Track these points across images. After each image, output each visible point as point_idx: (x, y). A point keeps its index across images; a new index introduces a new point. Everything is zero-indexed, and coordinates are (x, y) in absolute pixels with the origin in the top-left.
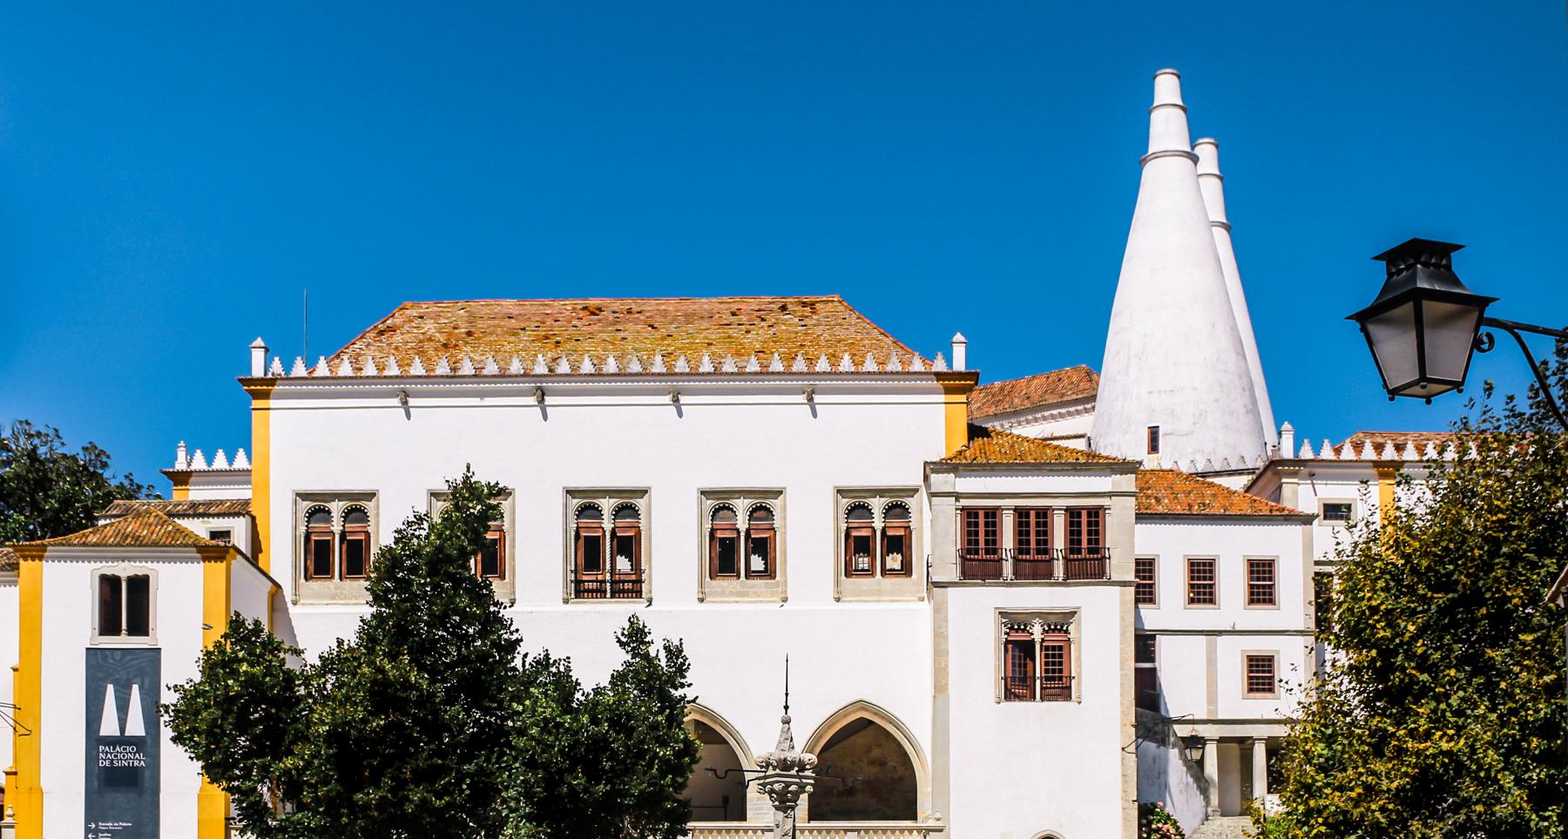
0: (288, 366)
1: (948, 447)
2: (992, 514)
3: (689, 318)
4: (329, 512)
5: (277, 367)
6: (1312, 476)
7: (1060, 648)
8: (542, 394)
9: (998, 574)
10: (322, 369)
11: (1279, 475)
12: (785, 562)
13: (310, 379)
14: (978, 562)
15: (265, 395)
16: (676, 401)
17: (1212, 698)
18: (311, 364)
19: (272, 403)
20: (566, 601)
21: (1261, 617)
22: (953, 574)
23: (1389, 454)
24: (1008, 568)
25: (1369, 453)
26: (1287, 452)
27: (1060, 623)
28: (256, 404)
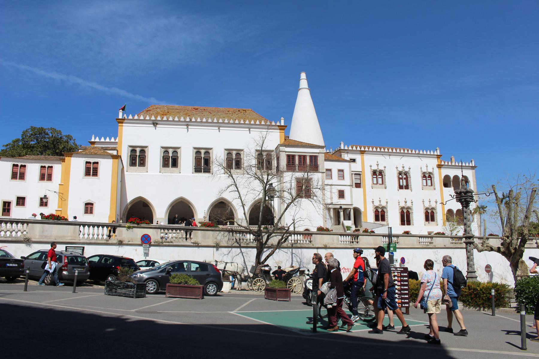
1: (280, 142)
2: (293, 156)
3: (218, 111)
5: (125, 115)
6: (347, 153)
8: (187, 125)
10: (136, 117)
11: (341, 152)
13: (133, 119)
15: (122, 123)
16: (219, 129)
18: (133, 116)
19: (124, 125)
21: (341, 182)
22: (285, 170)
23: (363, 149)
25: (358, 149)
26: (342, 148)
28: (120, 124)
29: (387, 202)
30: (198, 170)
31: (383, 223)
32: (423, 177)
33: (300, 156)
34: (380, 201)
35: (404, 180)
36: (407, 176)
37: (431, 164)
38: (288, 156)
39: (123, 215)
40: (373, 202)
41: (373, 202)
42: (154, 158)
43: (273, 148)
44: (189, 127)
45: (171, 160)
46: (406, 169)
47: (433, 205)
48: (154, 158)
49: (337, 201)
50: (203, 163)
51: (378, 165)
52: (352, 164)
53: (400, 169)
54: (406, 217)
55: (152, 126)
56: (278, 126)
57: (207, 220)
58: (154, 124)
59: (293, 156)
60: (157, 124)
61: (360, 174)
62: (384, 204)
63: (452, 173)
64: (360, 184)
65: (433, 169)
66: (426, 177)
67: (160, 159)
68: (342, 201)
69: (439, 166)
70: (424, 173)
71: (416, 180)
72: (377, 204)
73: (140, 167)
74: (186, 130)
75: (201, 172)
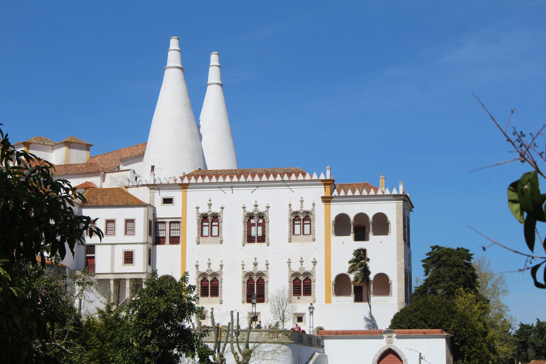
17: (112, 265)
29: (222, 266)
31: (214, 299)
32: (294, 220)
34: (209, 264)
35: (255, 228)
36: (264, 220)
37: (310, 196)
40: (197, 266)
41: (197, 266)
46: (261, 209)
47: (308, 267)
49: (121, 267)
51: (210, 205)
52: (168, 206)
53: (250, 209)
54: (255, 289)
61: (179, 222)
62: (215, 268)
63: (352, 210)
64: (179, 237)
65: (314, 205)
66: (300, 220)
68: (129, 268)
69: (327, 200)
70: (297, 213)
71: (278, 225)
72: (203, 268)
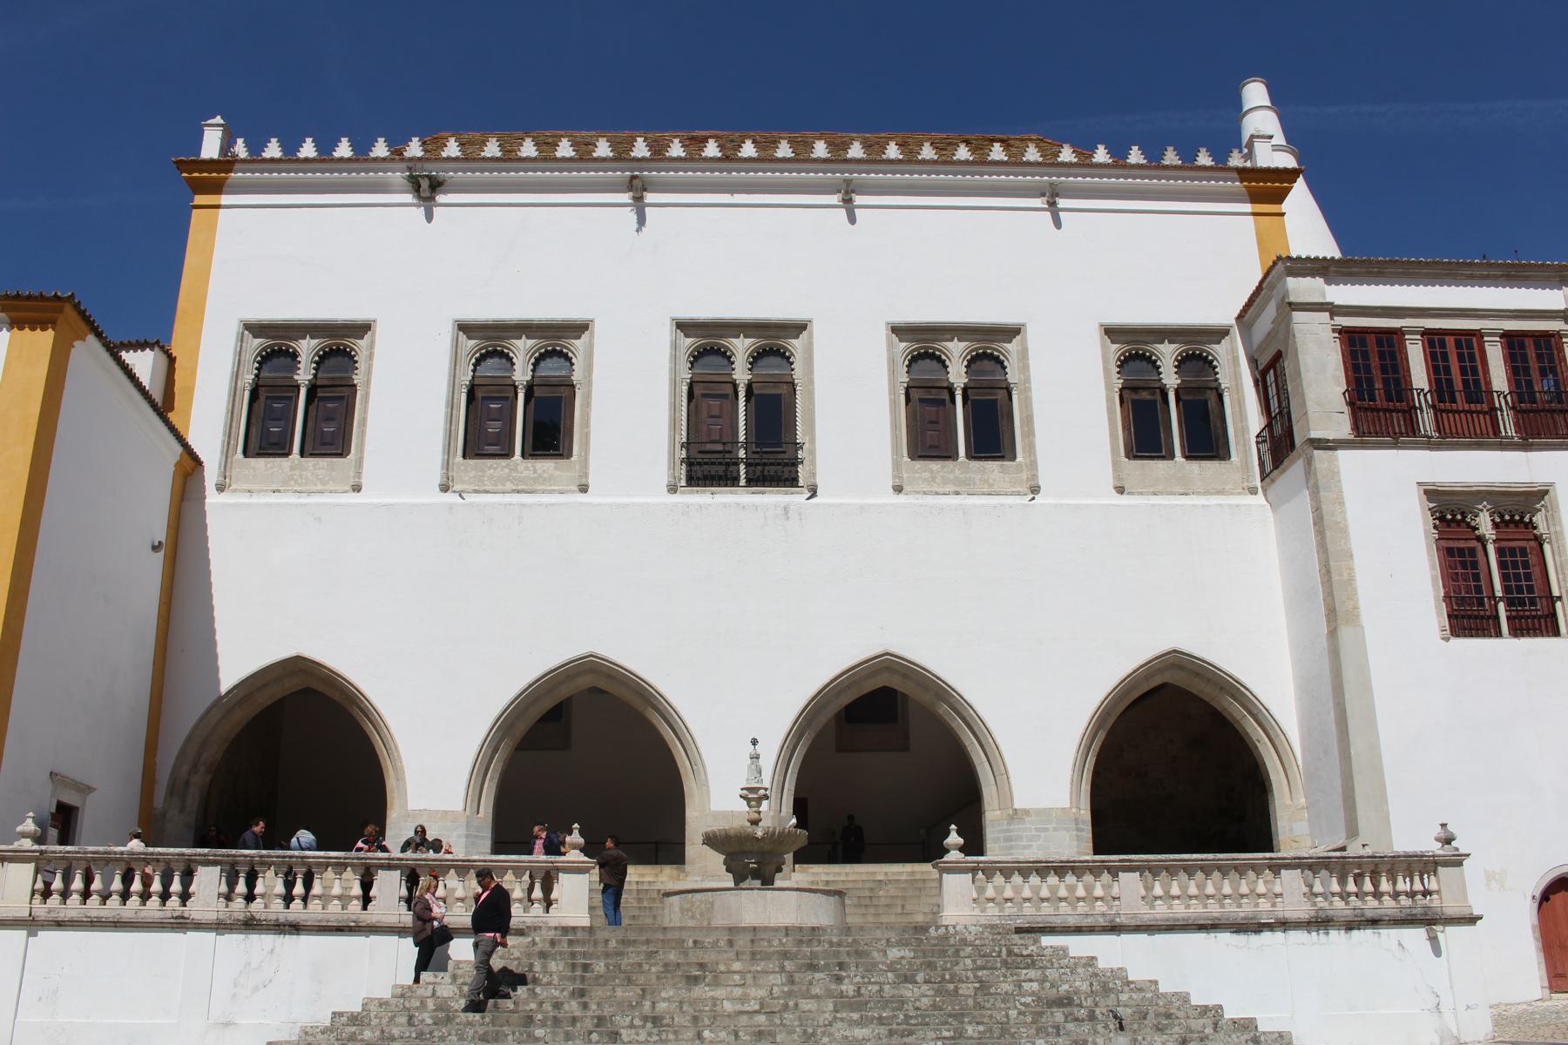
0: (256, 147)
2: (1390, 342)
4: (295, 355)
5: (240, 149)
7: (1523, 551)
9: (1412, 429)
12: (1030, 433)
14: (1380, 408)
15: (217, 188)
16: (847, 201)
19: (225, 199)
20: (673, 489)
22: (1341, 427)
24: (1426, 421)
27: (1519, 512)
28: (200, 199)
30: (706, 465)
33: (1433, 339)
38: (1352, 340)
39: (177, 788)
42: (408, 395)
43: (1223, 313)
44: (650, 198)
45: (520, 405)
48: (408, 395)
50: (742, 424)
55: (409, 198)
56: (1244, 174)
57: (778, 815)
58: (415, 185)
59: (1390, 342)
60: (436, 185)
67: (452, 405)
73: (311, 462)
74: (630, 216)
75: (729, 480)
